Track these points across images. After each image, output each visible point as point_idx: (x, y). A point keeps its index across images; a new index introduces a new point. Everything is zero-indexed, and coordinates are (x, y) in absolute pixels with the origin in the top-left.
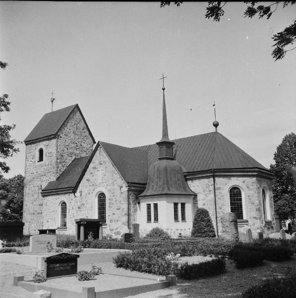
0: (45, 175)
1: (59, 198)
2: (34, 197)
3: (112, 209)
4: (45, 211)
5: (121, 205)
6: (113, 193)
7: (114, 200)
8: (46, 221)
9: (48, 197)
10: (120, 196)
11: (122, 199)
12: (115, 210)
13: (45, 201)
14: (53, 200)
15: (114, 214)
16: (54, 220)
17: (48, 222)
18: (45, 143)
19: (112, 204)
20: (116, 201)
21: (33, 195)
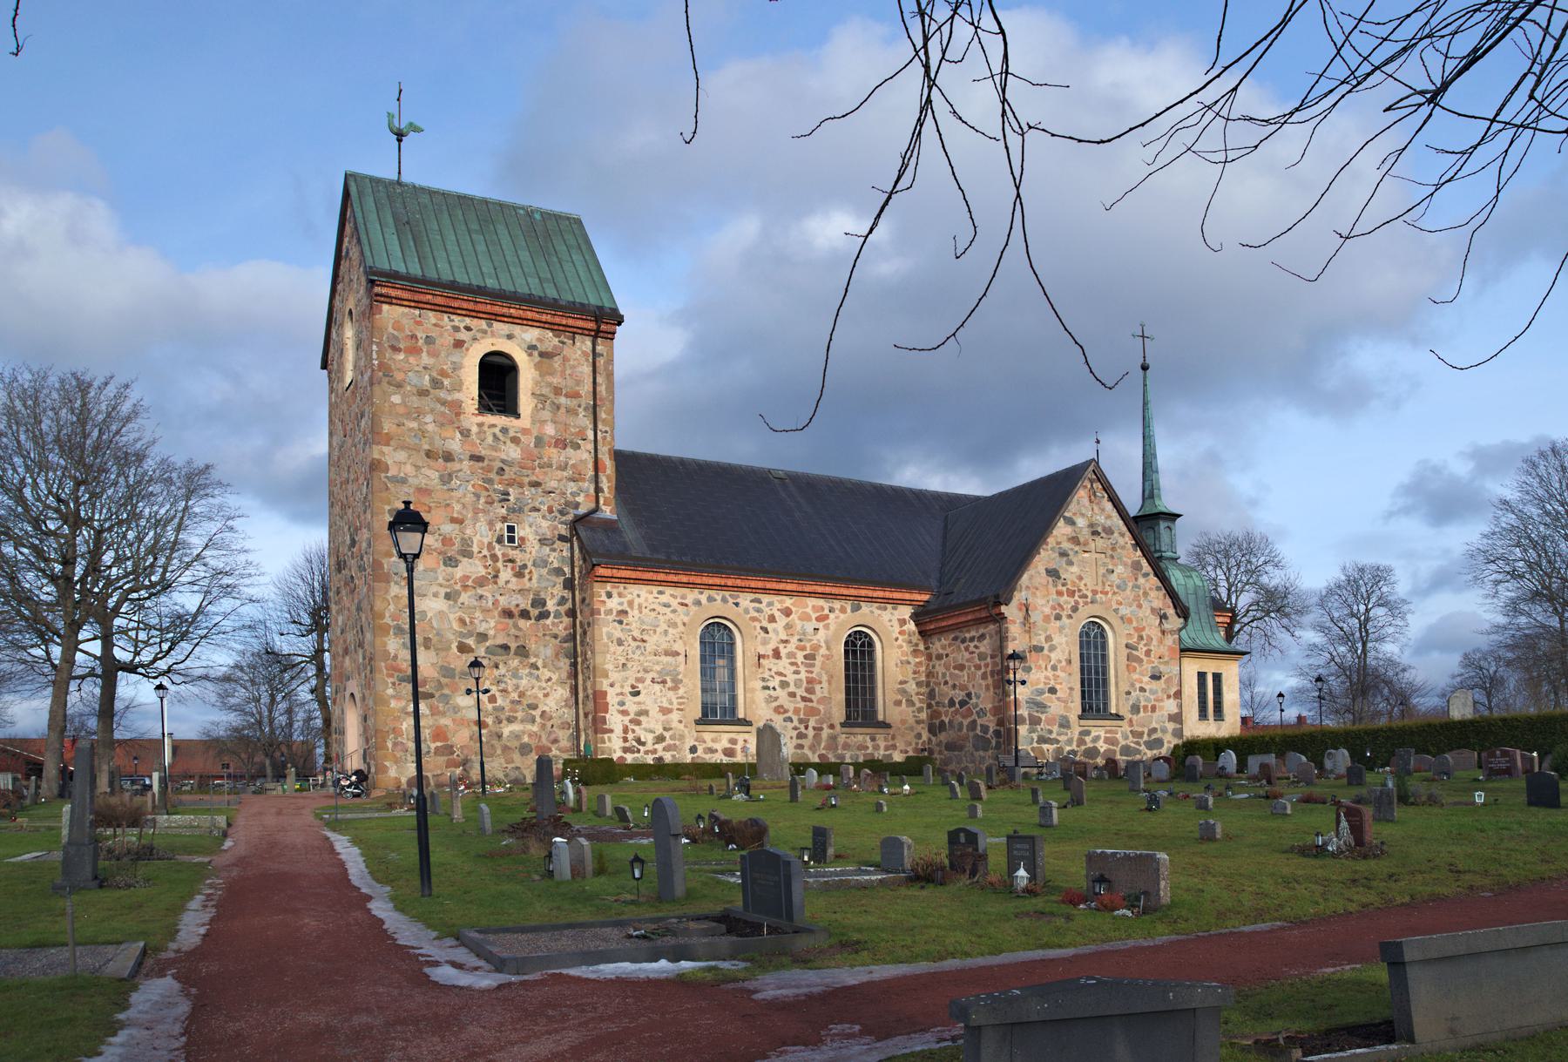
0: (536, 484)
1: (698, 603)
2: (459, 572)
3: (1135, 676)
4: (613, 647)
5: (1162, 668)
6: (1136, 629)
7: (1142, 648)
8: (628, 689)
9: (634, 590)
10: (1161, 642)
11: (1164, 650)
12: (1146, 679)
13: (614, 604)
14: (667, 605)
15: (1142, 690)
16: (675, 688)
17: (638, 693)
18: (531, 334)
19: (1140, 661)
20: (1148, 653)
21: (451, 562)
